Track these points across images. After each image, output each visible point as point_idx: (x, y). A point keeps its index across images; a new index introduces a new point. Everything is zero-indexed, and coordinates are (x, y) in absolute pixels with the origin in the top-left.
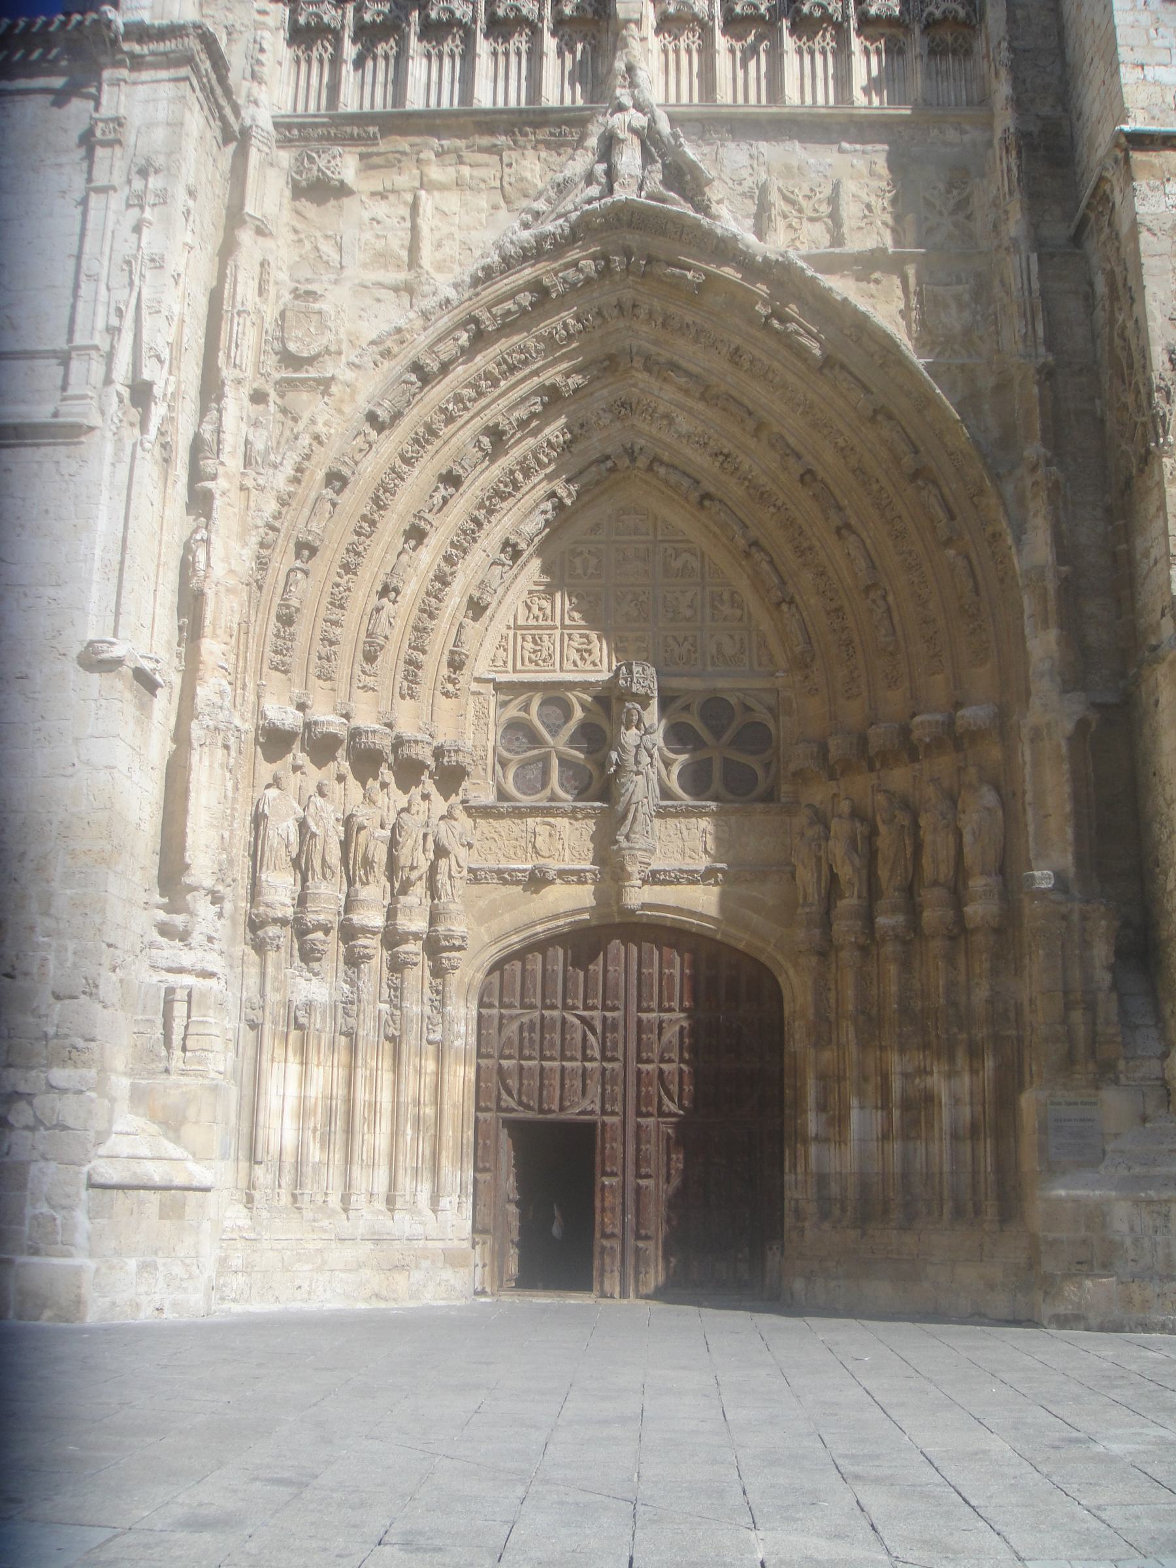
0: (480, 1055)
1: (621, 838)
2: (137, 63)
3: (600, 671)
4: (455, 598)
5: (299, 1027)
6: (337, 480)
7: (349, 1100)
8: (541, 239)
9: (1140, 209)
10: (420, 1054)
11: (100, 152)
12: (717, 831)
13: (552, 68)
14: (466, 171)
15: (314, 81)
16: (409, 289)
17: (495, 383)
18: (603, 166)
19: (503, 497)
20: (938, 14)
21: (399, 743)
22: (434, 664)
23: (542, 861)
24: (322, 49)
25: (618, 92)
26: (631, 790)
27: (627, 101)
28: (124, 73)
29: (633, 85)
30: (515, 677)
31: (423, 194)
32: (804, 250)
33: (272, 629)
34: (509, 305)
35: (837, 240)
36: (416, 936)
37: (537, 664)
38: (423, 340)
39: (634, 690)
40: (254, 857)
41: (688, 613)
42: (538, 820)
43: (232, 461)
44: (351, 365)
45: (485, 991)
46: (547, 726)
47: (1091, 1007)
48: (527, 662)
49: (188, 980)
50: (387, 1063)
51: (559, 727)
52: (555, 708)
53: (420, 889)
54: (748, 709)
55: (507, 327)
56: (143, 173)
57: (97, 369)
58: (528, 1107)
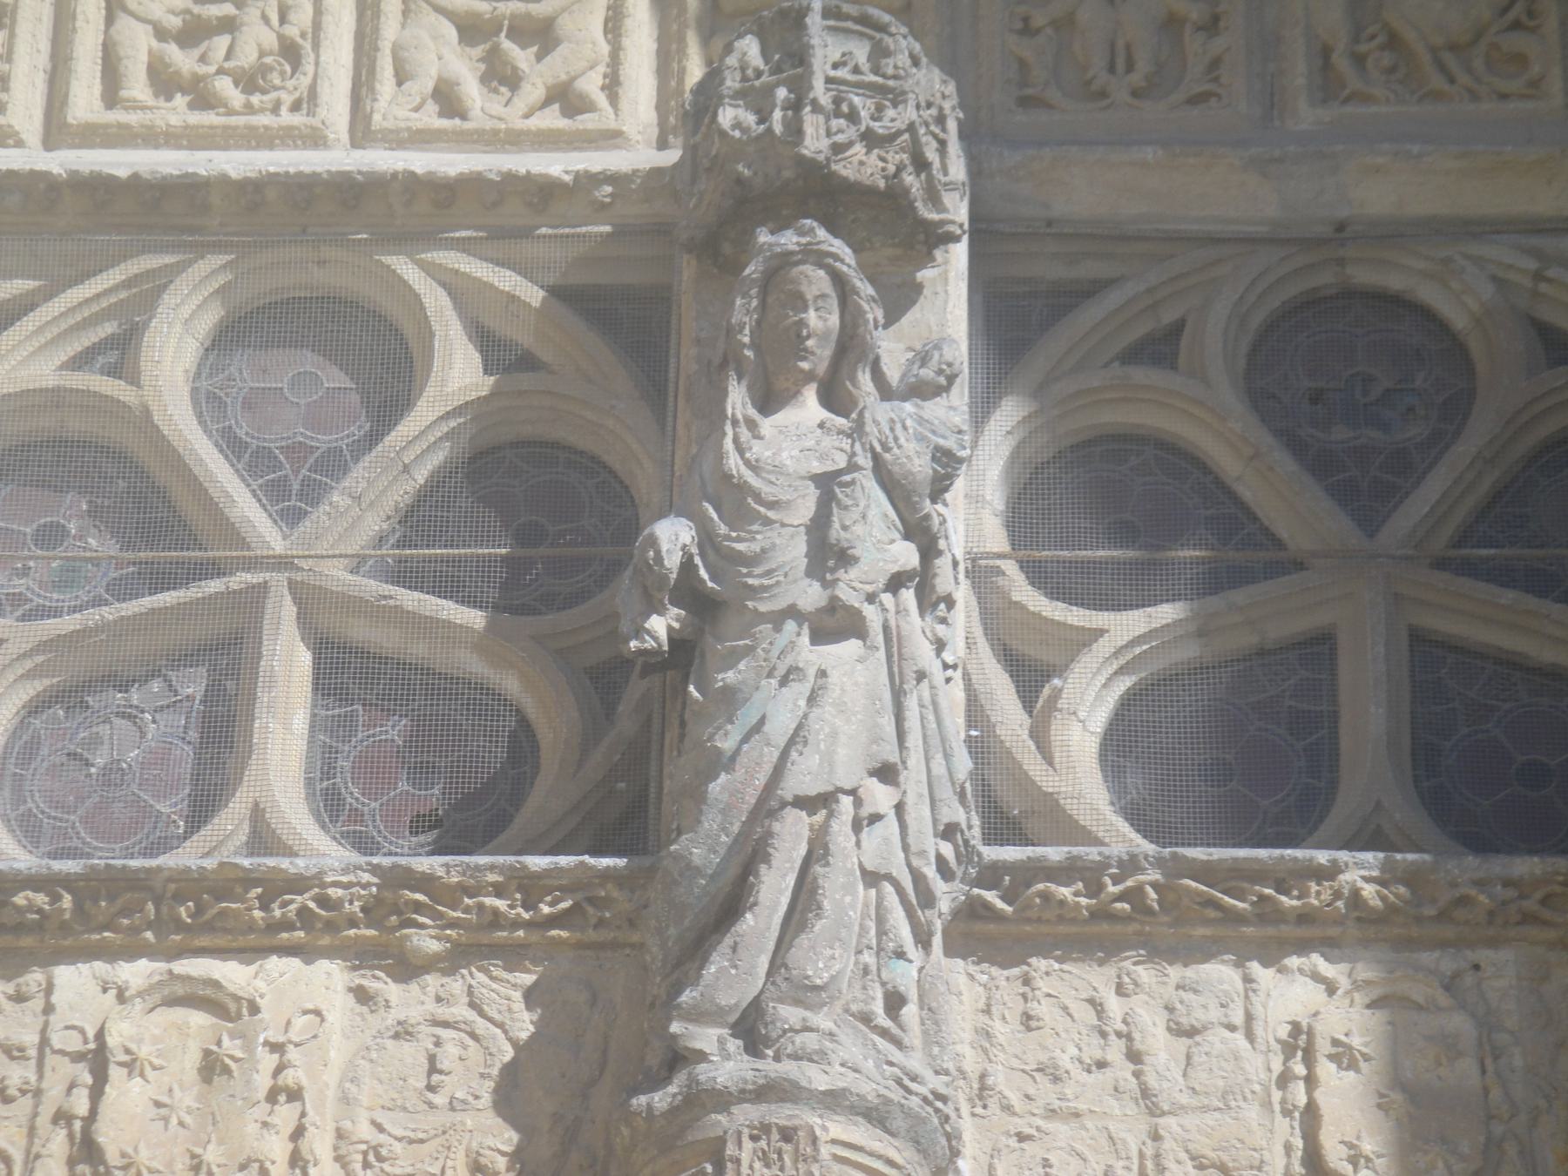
1: (707, 1038)
3: (611, 138)
12: (1397, 1045)
26: (781, 725)
37: (203, 99)
39: (815, 142)
42: (137, 972)
48: (137, 87)
51: (335, 464)
52: (308, 361)
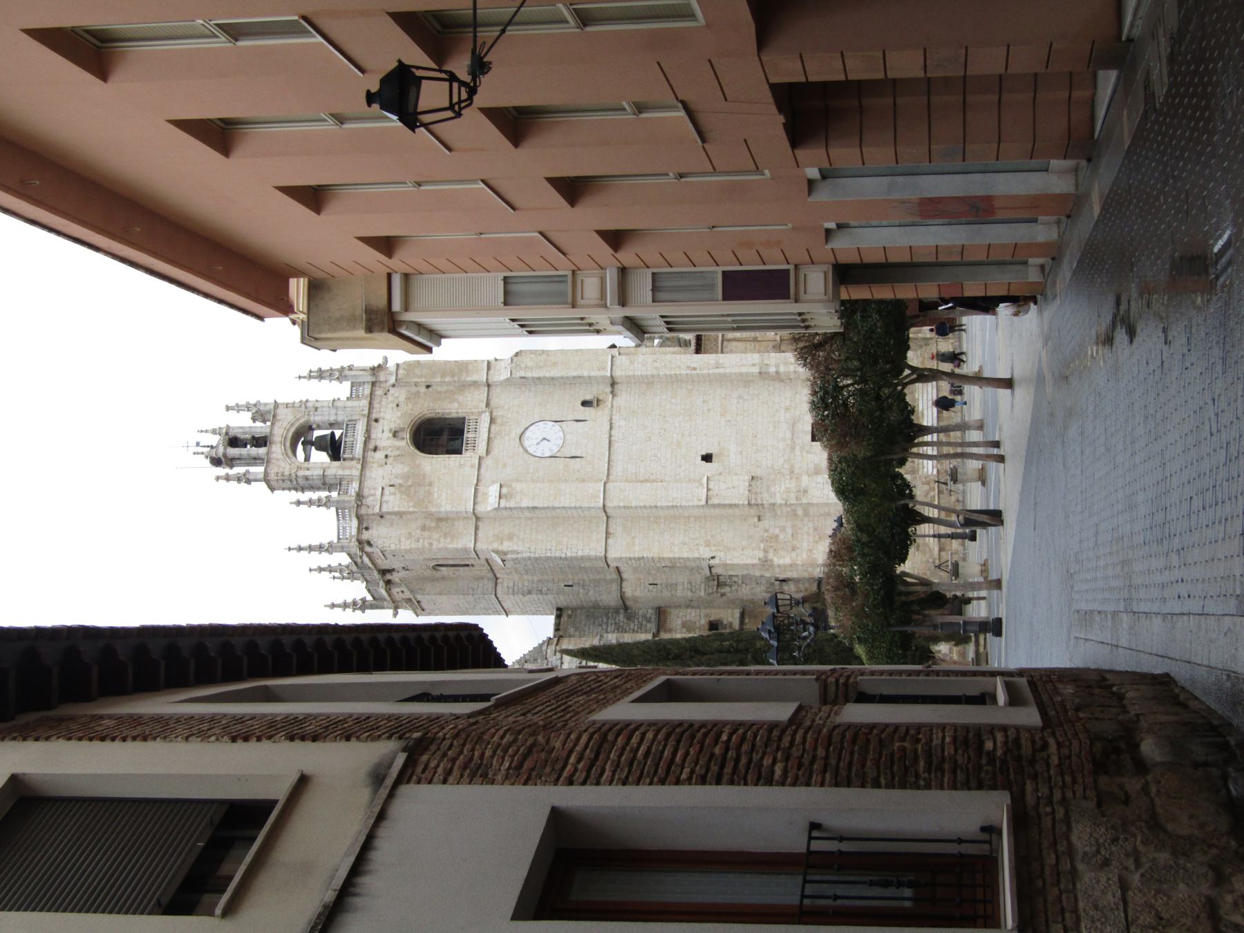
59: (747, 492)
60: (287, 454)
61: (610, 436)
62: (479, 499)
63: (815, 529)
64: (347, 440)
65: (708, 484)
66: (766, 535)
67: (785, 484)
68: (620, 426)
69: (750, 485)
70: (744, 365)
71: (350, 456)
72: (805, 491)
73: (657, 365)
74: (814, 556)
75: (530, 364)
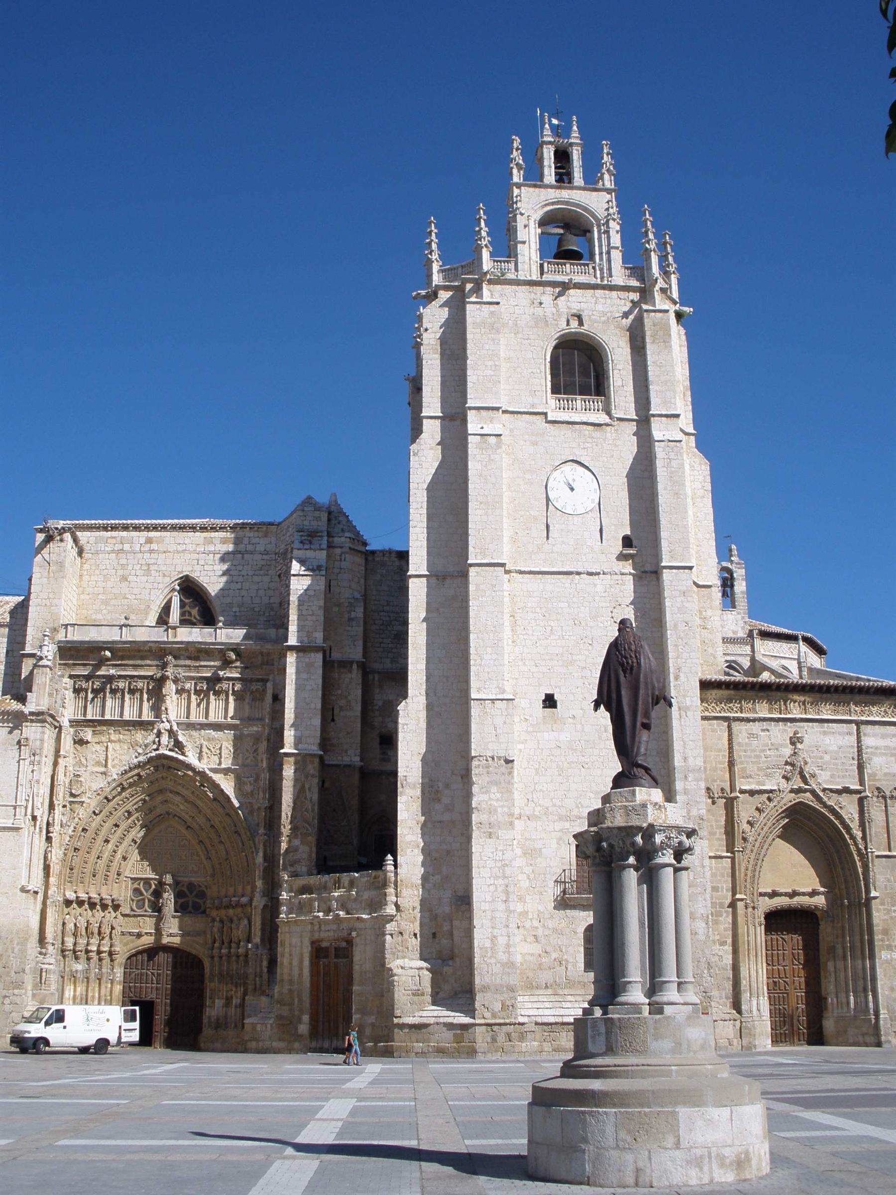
0: (124, 982)
2: (32, 721)
4: (119, 856)
5: (74, 977)
6: (84, 830)
7: (87, 995)
8: (139, 762)
9: (284, 774)
10: (107, 982)
11: (22, 747)
13: (146, 705)
14: (121, 736)
15: (80, 705)
16: (104, 773)
17: (128, 799)
18: (157, 739)
19: (132, 828)
20: (254, 690)
21: (102, 899)
22: (113, 875)
23: (141, 930)
24: (82, 695)
25: (163, 716)
27: (165, 720)
28: (29, 724)
29: (167, 714)
30: (136, 876)
31: (109, 744)
32: (209, 767)
33: (68, 872)
34: (131, 780)
35: (220, 764)
36: (105, 952)
38: (108, 790)
40: (63, 933)
41: (184, 858)
43: (56, 828)
44: (89, 798)
45: (126, 964)
46: (145, 889)
47: (261, 977)
49: (47, 966)
50: (97, 985)
53: (107, 938)
54: (200, 886)
55: (131, 785)
56: (34, 755)
57: (23, 810)
58: (136, 997)
59: (490, 755)
60: (546, 205)
61: (578, 573)
62: (483, 413)
63: (448, 852)
64: (568, 266)
65: (502, 700)
66: (440, 785)
67: (502, 806)
68: (595, 585)
69: (499, 758)
70: (685, 744)
71: (546, 270)
72: (490, 835)
73: (681, 626)
74: (409, 850)
75: (674, 464)
